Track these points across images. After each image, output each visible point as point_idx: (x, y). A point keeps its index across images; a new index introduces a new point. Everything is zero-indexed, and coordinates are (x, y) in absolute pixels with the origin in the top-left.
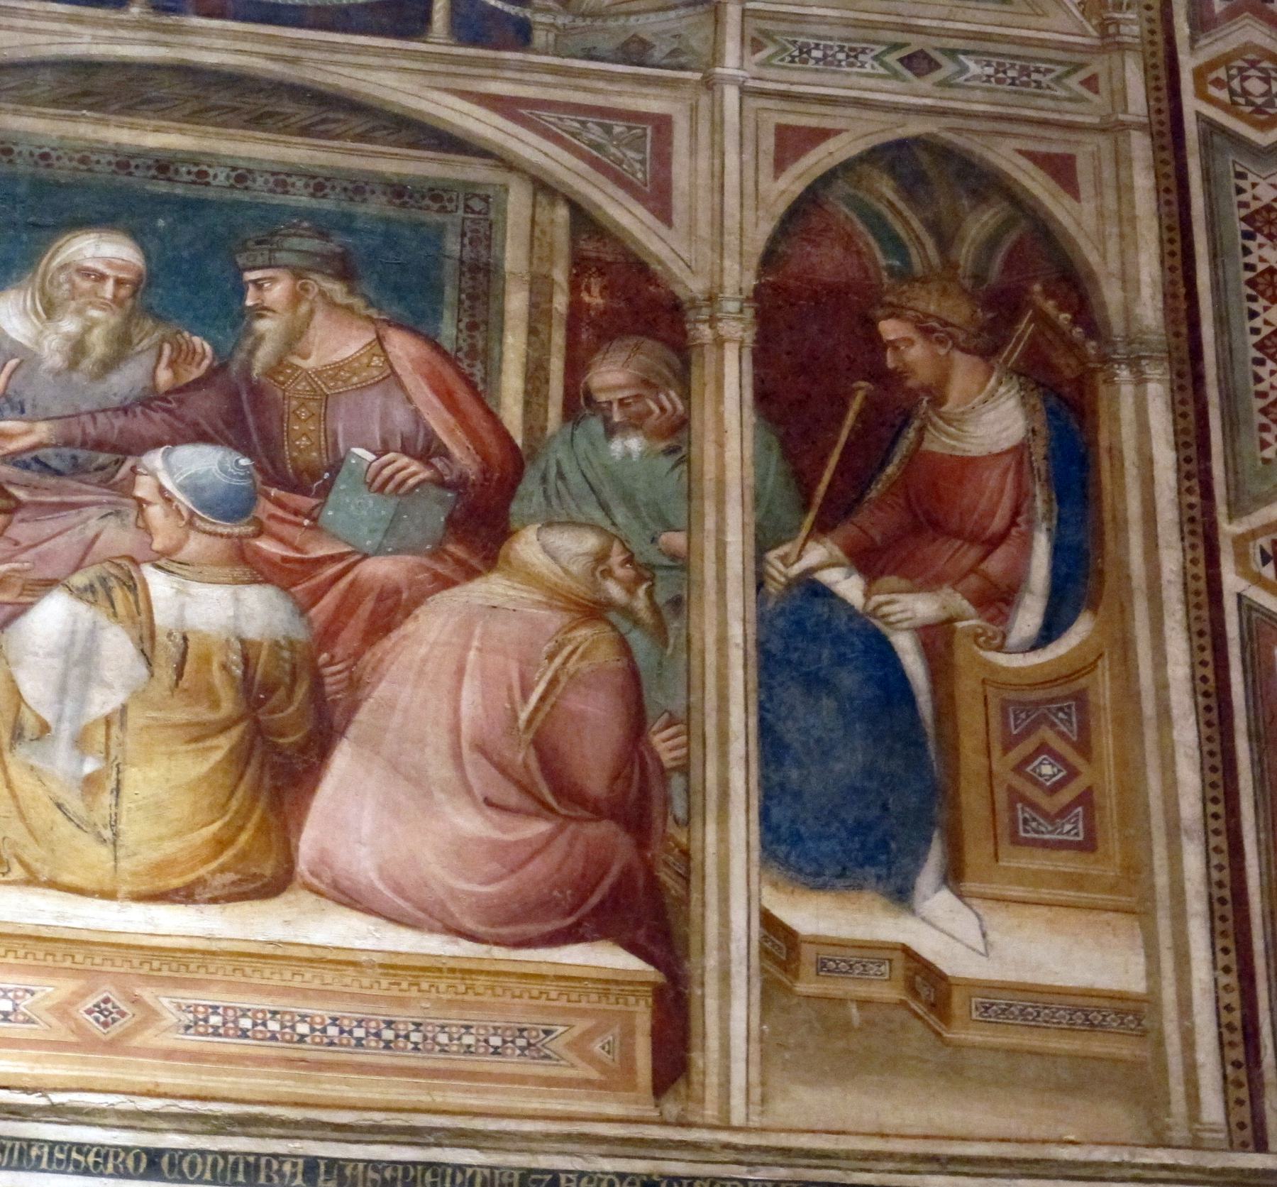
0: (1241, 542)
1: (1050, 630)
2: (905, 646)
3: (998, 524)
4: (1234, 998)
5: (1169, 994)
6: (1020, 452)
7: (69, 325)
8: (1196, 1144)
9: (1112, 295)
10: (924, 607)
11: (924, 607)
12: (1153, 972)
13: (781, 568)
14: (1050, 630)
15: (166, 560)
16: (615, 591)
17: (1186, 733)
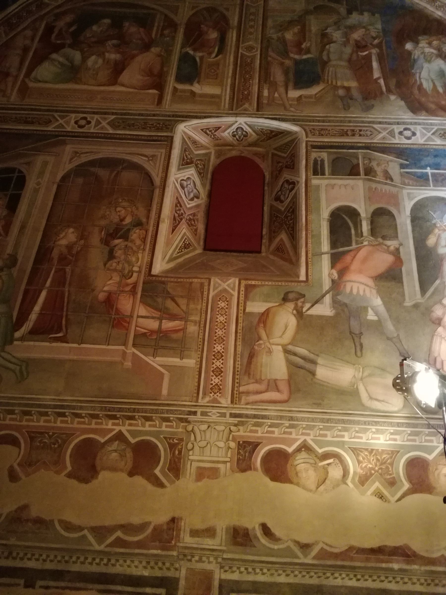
0: (242, 47)
1: (216, 56)
2: (198, 59)
3: (212, 45)
4: (232, 95)
5: (223, 94)
6: (216, 38)
7: (101, 28)
8: (224, 110)
9: (231, 22)
10: (201, 54)
11: (201, 54)
12: (222, 92)
13: (184, 50)
14: (216, 56)
15: (108, 52)
16: (162, 53)
17: (231, 67)
